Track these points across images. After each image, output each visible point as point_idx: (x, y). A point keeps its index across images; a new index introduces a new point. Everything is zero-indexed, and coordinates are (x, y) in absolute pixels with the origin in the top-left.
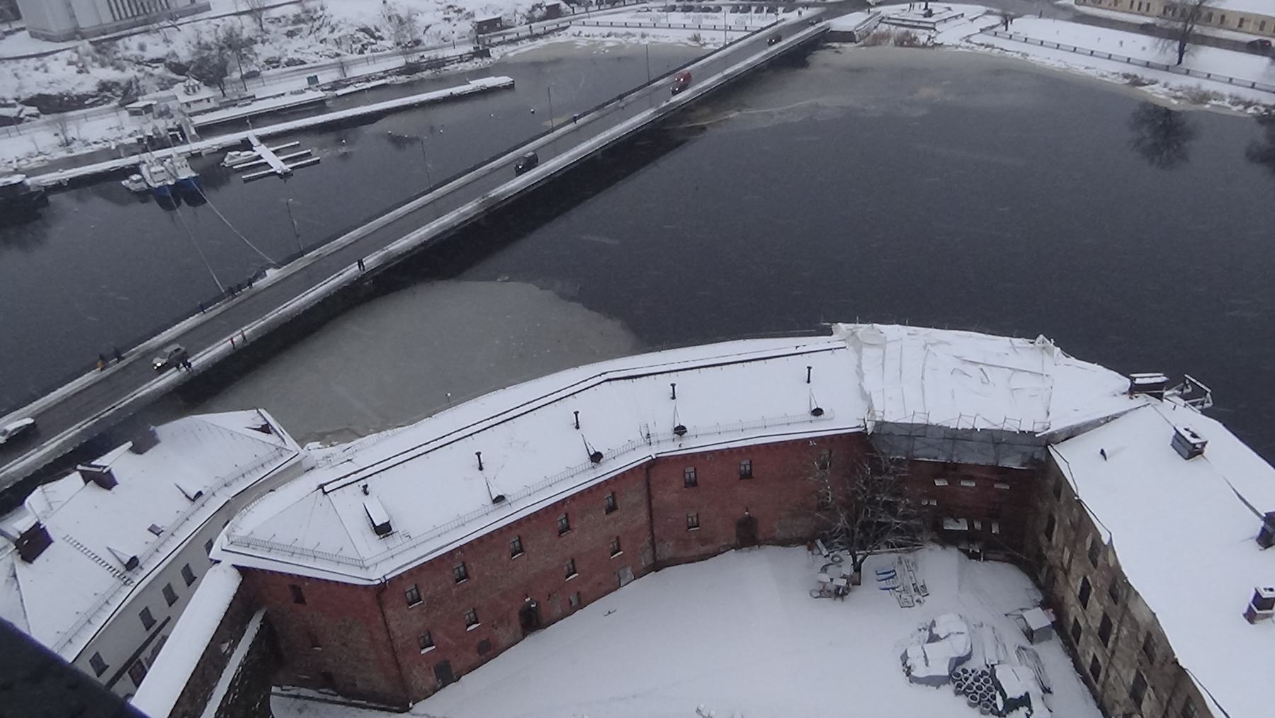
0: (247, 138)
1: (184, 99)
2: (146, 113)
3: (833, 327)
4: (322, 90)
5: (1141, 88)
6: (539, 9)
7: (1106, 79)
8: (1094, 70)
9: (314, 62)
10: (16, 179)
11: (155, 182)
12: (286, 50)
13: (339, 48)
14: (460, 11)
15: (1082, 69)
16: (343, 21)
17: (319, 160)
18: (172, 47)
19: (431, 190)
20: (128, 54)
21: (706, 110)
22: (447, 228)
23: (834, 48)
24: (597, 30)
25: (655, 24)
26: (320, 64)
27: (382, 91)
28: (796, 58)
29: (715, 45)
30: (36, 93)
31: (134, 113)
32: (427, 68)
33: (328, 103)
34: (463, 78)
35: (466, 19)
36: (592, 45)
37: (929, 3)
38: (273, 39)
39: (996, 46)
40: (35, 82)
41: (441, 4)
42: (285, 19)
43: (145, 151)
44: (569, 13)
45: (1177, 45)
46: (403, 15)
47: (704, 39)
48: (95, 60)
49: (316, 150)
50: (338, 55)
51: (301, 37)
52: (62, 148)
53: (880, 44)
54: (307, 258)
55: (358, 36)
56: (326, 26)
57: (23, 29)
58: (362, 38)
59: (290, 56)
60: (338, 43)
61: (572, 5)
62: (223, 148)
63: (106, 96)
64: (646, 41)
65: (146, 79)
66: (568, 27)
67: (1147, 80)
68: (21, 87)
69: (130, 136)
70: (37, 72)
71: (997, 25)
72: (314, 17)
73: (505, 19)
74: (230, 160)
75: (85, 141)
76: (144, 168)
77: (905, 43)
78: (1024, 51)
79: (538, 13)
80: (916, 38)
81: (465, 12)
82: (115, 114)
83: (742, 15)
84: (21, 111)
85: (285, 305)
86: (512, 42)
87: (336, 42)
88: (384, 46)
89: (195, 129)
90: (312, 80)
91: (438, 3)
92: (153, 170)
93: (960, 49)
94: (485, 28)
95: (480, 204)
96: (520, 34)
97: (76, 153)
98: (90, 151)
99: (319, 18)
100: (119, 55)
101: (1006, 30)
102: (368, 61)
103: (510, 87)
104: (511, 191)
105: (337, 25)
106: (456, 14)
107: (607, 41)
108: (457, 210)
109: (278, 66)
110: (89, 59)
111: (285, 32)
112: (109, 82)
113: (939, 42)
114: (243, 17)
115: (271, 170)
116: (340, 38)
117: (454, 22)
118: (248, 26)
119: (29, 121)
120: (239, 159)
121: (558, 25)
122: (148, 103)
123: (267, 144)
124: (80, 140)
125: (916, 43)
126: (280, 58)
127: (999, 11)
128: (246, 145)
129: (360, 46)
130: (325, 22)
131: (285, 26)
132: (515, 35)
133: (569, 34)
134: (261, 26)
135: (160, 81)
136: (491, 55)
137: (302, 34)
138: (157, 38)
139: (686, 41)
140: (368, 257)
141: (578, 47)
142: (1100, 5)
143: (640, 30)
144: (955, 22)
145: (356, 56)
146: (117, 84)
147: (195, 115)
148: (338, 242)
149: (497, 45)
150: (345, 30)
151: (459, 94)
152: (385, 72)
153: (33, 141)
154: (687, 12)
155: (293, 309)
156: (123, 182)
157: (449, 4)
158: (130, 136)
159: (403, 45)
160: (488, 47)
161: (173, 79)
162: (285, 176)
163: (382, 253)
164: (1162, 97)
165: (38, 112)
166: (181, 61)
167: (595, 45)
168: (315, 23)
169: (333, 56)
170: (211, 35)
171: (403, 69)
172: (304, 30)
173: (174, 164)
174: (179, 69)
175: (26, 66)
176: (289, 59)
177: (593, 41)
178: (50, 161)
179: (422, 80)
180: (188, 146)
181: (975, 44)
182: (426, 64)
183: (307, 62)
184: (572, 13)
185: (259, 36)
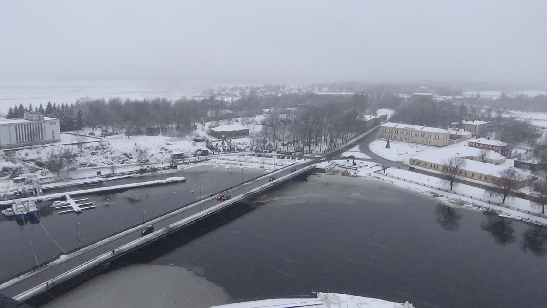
0: (65, 195)
1: (40, 177)
2: (21, 182)
3: (317, 294)
4: (102, 177)
5: (438, 198)
6: (199, 151)
7: (424, 193)
8: (419, 190)
9: (101, 166)
11: (18, 212)
13: (113, 161)
14: (166, 150)
15: (414, 189)
16: (116, 150)
17: (95, 207)
18: (40, 155)
19: (144, 223)
20: (19, 157)
21: (265, 196)
22: (148, 240)
23: (317, 174)
24: (222, 161)
25: (246, 161)
28: (302, 177)
29: (270, 170)
33: (104, 183)
35: (169, 153)
37: (354, 160)
38: (85, 155)
39: (381, 178)
42: (92, 148)
43: (17, 198)
44: (212, 154)
45: (450, 182)
46: (143, 150)
47: (266, 168)
48: (4, 158)
51: (97, 155)
53: (336, 174)
54: (82, 250)
55: (122, 156)
56: (109, 152)
59: (91, 163)
60: (113, 159)
61: (213, 151)
62: (53, 199)
63: (5, 174)
64: (242, 167)
66: (211, 159)
67: (440, 195)
69: (12, 191)
71: (381, 170)
72: (105, 148)
74: (55, 204)
76: (14, 206)
77: (346, 175)
78: (392, 181)
79: (199, 153)
80: (349, 173)
81: (169, 150)
82: (7, 181)
83: (282, 159)
85: (66, 273)
86: (187, 163)
87: (112, 158)
88: (132, 161)
89: (42, 190)
90: (99, 173)
91: (158, 146)
92: (18, 207)
93: (367, 178)
94: (176, 157)
95: (165, 230)
96: (190, 161)
99: (106, 148)
100: (15, 157)
101: (384, 172)
102: (124, 167)
103: (184, 181)
104: (179, 225)
105: (114, 152)
106: (165, 151)
109: (84, 167)
111: (91, 153)
112: (8, 168)
113: (359, 175)
114: (74, 145)
115: (73, 210)
116: (114, 157)
118: (75, 149)
120: (59, 204)
121: (207, 158)
123: (73, 198)
125: (350, 175)
126: (86, 163)
128: (64, 198)
130: (109, 150)
131: (91, 150)
133: (211, 162)
134: (81, 149)
135: (30, 169)
136: (177, 168)
137: (98, 154)
138: (34, 151)
139: (258, 168)
141: (214, 167)
142: (419, 165)
144: (364, 168)
145: (119, 165)
146: (11, 169)
147: (43, 184)
148: (97, 244)
149: (180, 164)
150: (117, 154)
154: (259, 157)
155: (70, 274)
157: (163, 147)
158: (12, 191)
159: (141, 161)
160: (176, 165)
161: (38, 168)
162: (79, 213)
164: (446, 202)
166: (42, 161)
167: (221, 167)
168: (105, 150)
170: (58, 152)
171: (140, 171)
172: (99, 152)
174: (41, 164)
176: (91, 164)
177: (220, 165)
179: (147, 176)
181: (373, 177)
182: (149, 170)
183: (98, 165)
184: (213, 154)
185: (80, 154)
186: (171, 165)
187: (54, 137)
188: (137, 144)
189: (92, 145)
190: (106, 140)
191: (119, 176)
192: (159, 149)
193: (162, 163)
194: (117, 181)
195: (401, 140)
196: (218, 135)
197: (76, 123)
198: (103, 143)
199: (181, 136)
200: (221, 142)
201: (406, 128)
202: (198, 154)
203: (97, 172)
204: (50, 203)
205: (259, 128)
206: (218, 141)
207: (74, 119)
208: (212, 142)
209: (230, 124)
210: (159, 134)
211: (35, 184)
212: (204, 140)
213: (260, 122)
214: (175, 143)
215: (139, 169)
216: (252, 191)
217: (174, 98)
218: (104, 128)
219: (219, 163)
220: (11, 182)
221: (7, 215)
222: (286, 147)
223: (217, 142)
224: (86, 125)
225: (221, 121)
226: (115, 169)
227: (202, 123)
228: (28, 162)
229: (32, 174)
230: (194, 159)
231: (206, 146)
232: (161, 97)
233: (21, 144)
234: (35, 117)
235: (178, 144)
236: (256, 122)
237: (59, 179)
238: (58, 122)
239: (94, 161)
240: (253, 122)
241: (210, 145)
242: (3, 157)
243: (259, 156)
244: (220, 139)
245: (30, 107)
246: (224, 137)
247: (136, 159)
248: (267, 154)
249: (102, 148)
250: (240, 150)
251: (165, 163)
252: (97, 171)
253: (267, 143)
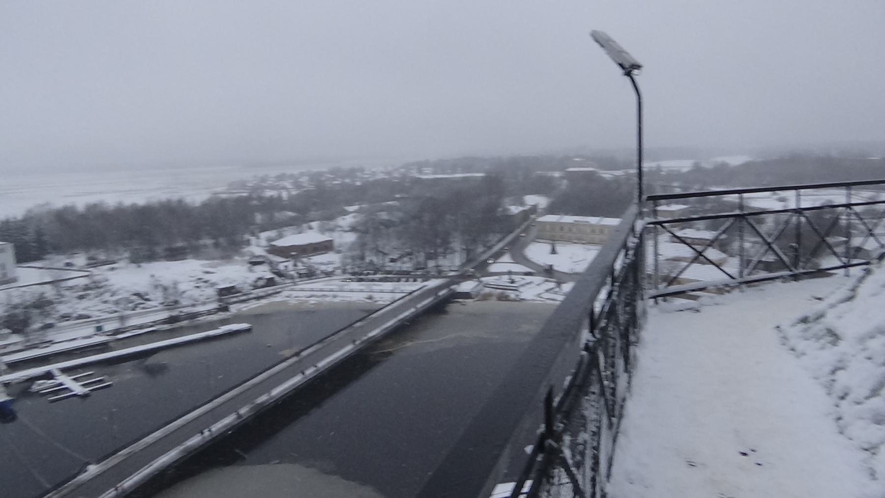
14: (206, 282)
21: (390, 342)
23: (461, 302)
27: (153, 335)
32: (185, 319)
33: (111, 344)
34: (212, 325)
35: (212, 287)
50: (116, 312)
60: (117, 303)
64: (337, 300)
79: (261, 283)
90: (99, 329)
94: (224, 292)
95: (251, 408)
103: (248, 331)
107: (310, 300)
127: (555, 280)
128: (49, 376)
141: (291, 304)
147: (4, 355)
162: (85, 396)
167: (302, 303)
171: (167, 320)
179: (181, 328)
190: (100, 273)
193: (204, 304)
195: (569, 241)
196: (284, 252)
198: (97, 278)
201: (576, 221)
204: (26, 384)
205: (350, 238)
209: (300, 233)
214: (219, 270)
217: (196, 197)
222: (398, 264)
227: (253, 234)
232: (175, 197)
243: (361, 280)
249: (95, 287)
250: (328, 274)
253: (368, 260)
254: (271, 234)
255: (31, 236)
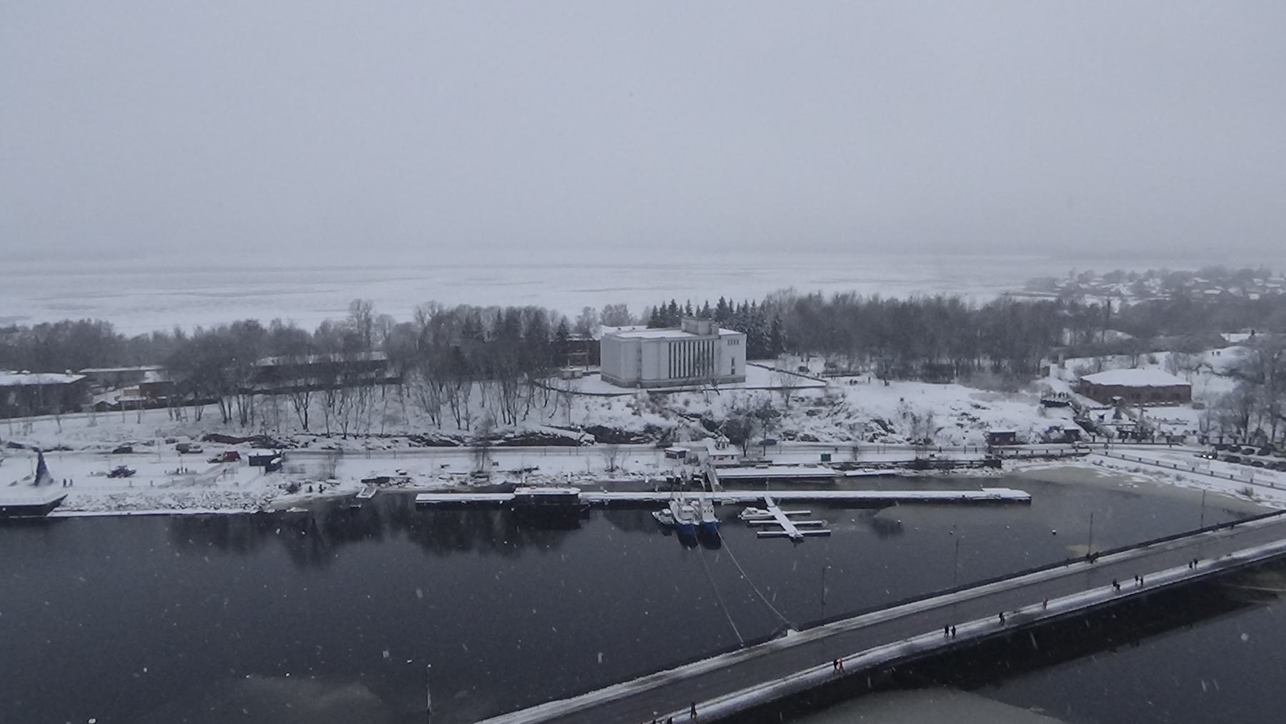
1: (713, 452)
2: (680, 457)
6: (1056, 431)
9: (826, 441)
10: (573, 491)
12: (804, 427)
13: (851, 433)
14: (974, 420)
16: (860, 410)
17: (829, 533)
18: (710, 407)
19: (954, 591)
20: (674, 406)
24: (1122, 464)
25: (1193, 469)
26: (830, 444)
30: (598, 424)
31: (669, 456)
32: (935, 467)
33: (837, 481)
34: (974, 483)
35: (980, 428)
36: (1118, 477)
40: (600, 415)
41: (956, 410)
47: (1257, 495)
48: (648, 406)
49: (826, 522)
51: (819, 418)
52: (606, 473)
54: (827, 628)
56: (843, 412)
57: (598, 373)
58: (875, 428)
59: (806, 433)
60: (852, 428)
62: (740, 502)
64: (1183, 485)
65: (683, 428)
68: (588, 417)
70: (603, 408)
72: (836, 402)
73: (1019, 434)
75: (626, 470)
76: (672, 504)
79: (1054, 435)
82: (653, 453)
84: (583, 436)
85: (806, 671)
86: (1024, 457)
88: (893, 439)
90: (826, 458)
91: (953, 409)
92: (684, 508)
95: (1013, 618)
97: (616, 479)
98: (627, 480)
99: (838, 404)
100: (667, 406)
102: (878, 450)
103: (1027, 502)
106: (969, 422)
107: (1134, 476)
108: (986, 619)
110: (644, 404)
111: (807, 411)
112: (654, 426)
114: (773, 392)
115: (784, 532)
116: (854, 424)
117: (967, 428)
119: (586, 445)
120: (755, 515)
122: (683, 449)
124: (622, 469)
126: (797, 432)
128: (761, 504)
129: (872, 435)
131: (806, 406)
132: (1028, 453)
134: (787, 402)
136: (1002, 466)
137: (820, 415)
138: (700, 397)
140: (891, 644)
141: (1100, 476)
143: (1175, 472)
145: (865, 443)
146: (660, 429)
149: (1009, 458)
151: (971, 498)
152: (893, 463)
153: (588, 462)
156: (653, 513)
157: (963, 411)
158: (662, 474)
159: (913, 441)
160: (1000, 459)
162: (796, 540)
163: (905, 644)
165: (594, 439)
166: (714, 420)
168: (835, 408)
169: (845, 439)
173: (703, 507)
174: (711, 426)
175: (596, 402)
176: (805, 435)
178: (596, 482)
179: (929, 478)
180: (711, 493)
184: (1092, 441)
186: (987, 457)
187: (733, 372)
188: (905, 400)
189: (807, 395)
190: (839, 385)
191: (866, 470)
192: (956, 416)
193: (965, 450)
194: (861, 481)
196: (1103, 394)
197: (768, 344)
198: (831, 392)
199: (1009, 389)
200: (1113, 411)
202: (1052, 438)
203: (822, 456)
204: (738, 508)
205: (1226, 386)
206: (1104, 409)
207: (765, 334)
208: (1088, 410)
209: (1134, 367)
210: (952, 381)
211: (703, 466)
212: (1069, 405)
213: (1224, 367)
214: (993, 406)
215: (912, 460)
216: (1236, 555)
217: (977, 297)
218: (831, 359)
219: (1111, 467)
220: (662, 455)
221: (662, 521)
223: (1101, 412)
224: (788, 349)
225: (1109, 357)
226: (860, 454)
227: (1055, 359)
228: (688, 419)
229: (694, 444)
230: (1029, 450)
231: (1074, 418)
233: (675, 380)
234: (703, 326)
235: (1001, 409)
236: (1211, 368)
237: (746, 462)
238: (743, 339)
239: (812, 429)
240: (1200, 366)
241: (1085, 419)
242: (647, 404)
243: (1237, 460)
244: (1108, 406)
245: (688, 309)
246: (1121, 400)
247: (901, 433)
248: (1253, 457)
249: (829, 403)
250: (1171, 440)
251: (971, 450)
252: (822, 453)
253: (1253, 427)
254: (1087, 363)
255: (767, 328)
